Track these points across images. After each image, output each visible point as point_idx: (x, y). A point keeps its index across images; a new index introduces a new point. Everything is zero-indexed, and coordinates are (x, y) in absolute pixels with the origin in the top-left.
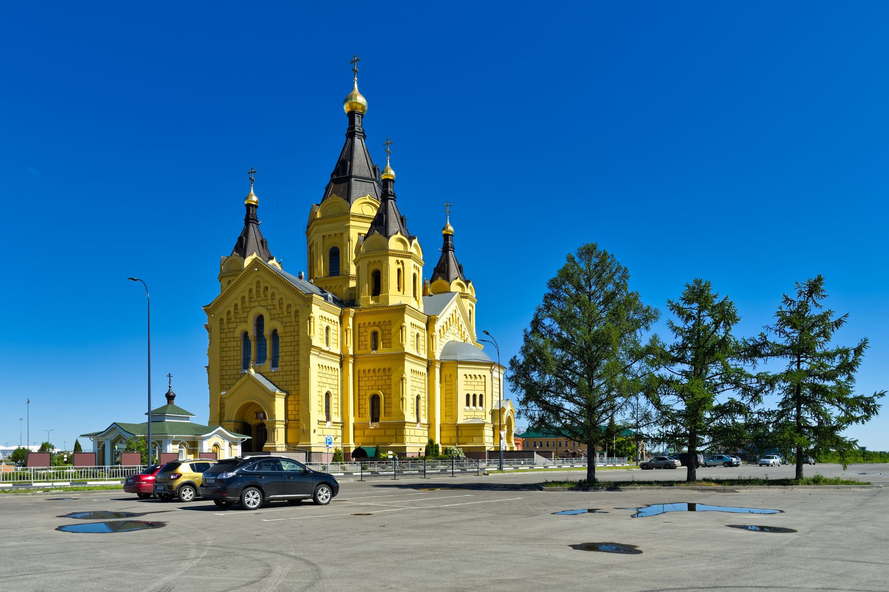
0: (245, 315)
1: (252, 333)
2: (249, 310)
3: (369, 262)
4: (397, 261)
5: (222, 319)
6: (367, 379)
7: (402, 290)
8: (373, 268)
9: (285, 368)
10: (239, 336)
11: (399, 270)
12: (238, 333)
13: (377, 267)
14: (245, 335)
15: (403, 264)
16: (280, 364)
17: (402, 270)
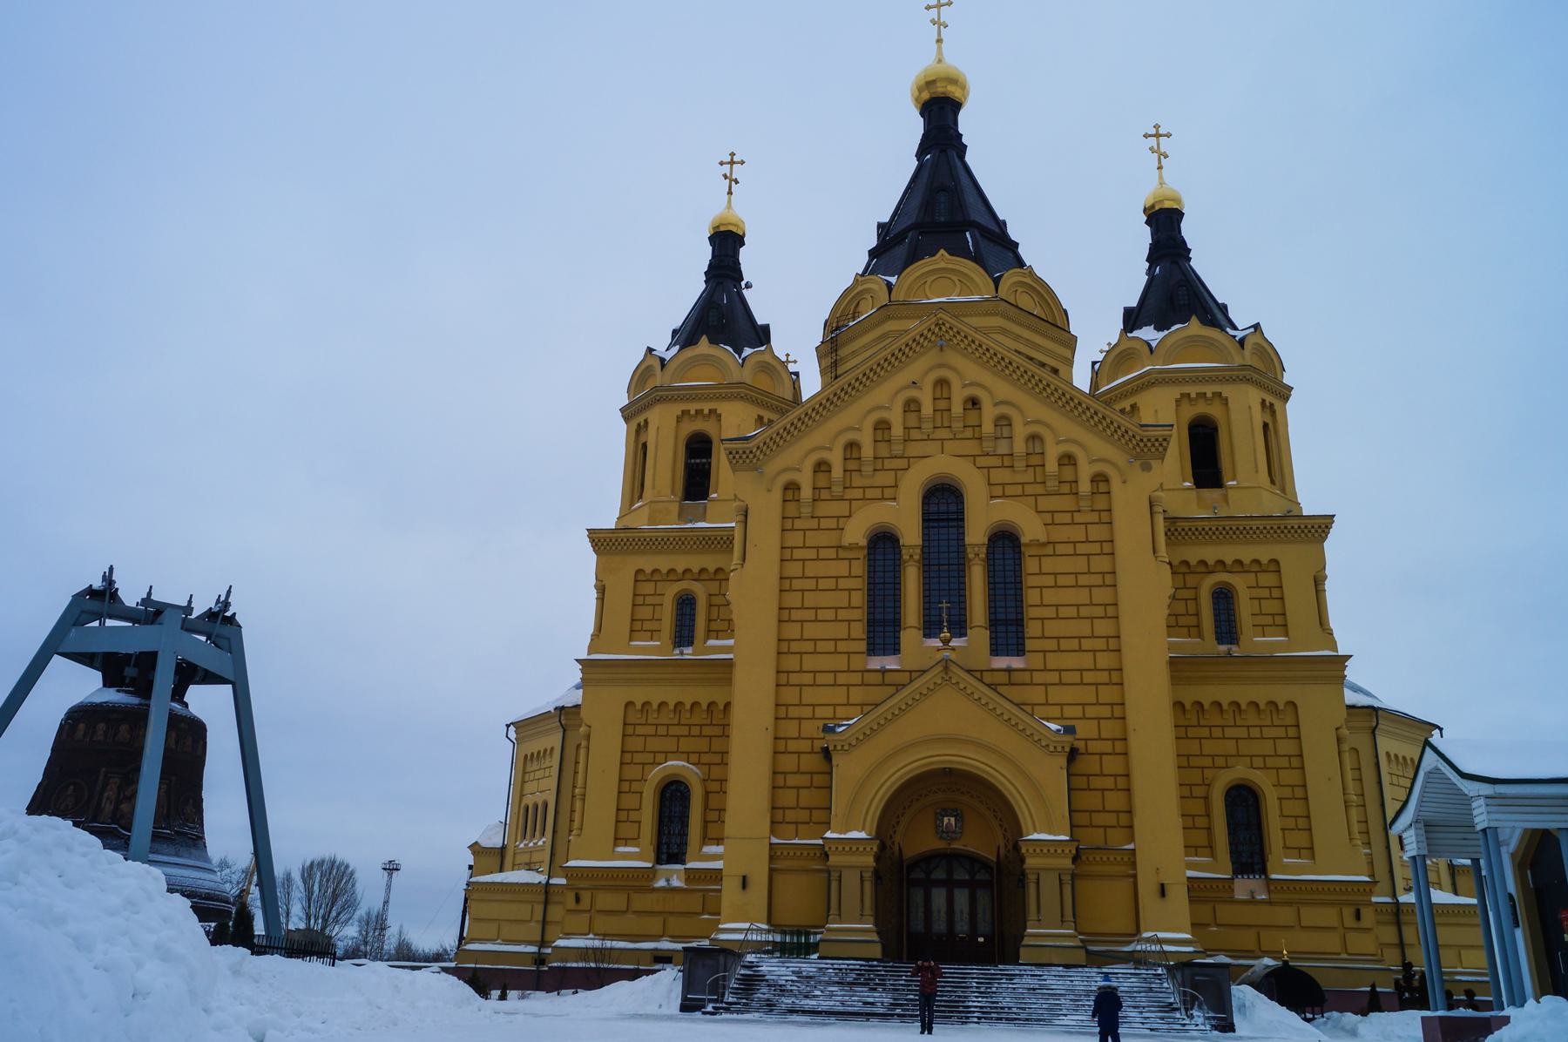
0: (885, 478)
1: (911, 534)
2: (902, 463)
3: (1181, 394)
4: (1264, 401)
5: (792, 487)
6: (1205, 732)
7: (1277, 479)
8: (1189, 412)
9: (1054, 661)
10: (863, 542)
11: (1265, 426)
12: (857, 532)
13: (1201, 408)
14: (883, 542)
15: (1273, 413)
16: (1029, 645)
17: (1271, 426)
